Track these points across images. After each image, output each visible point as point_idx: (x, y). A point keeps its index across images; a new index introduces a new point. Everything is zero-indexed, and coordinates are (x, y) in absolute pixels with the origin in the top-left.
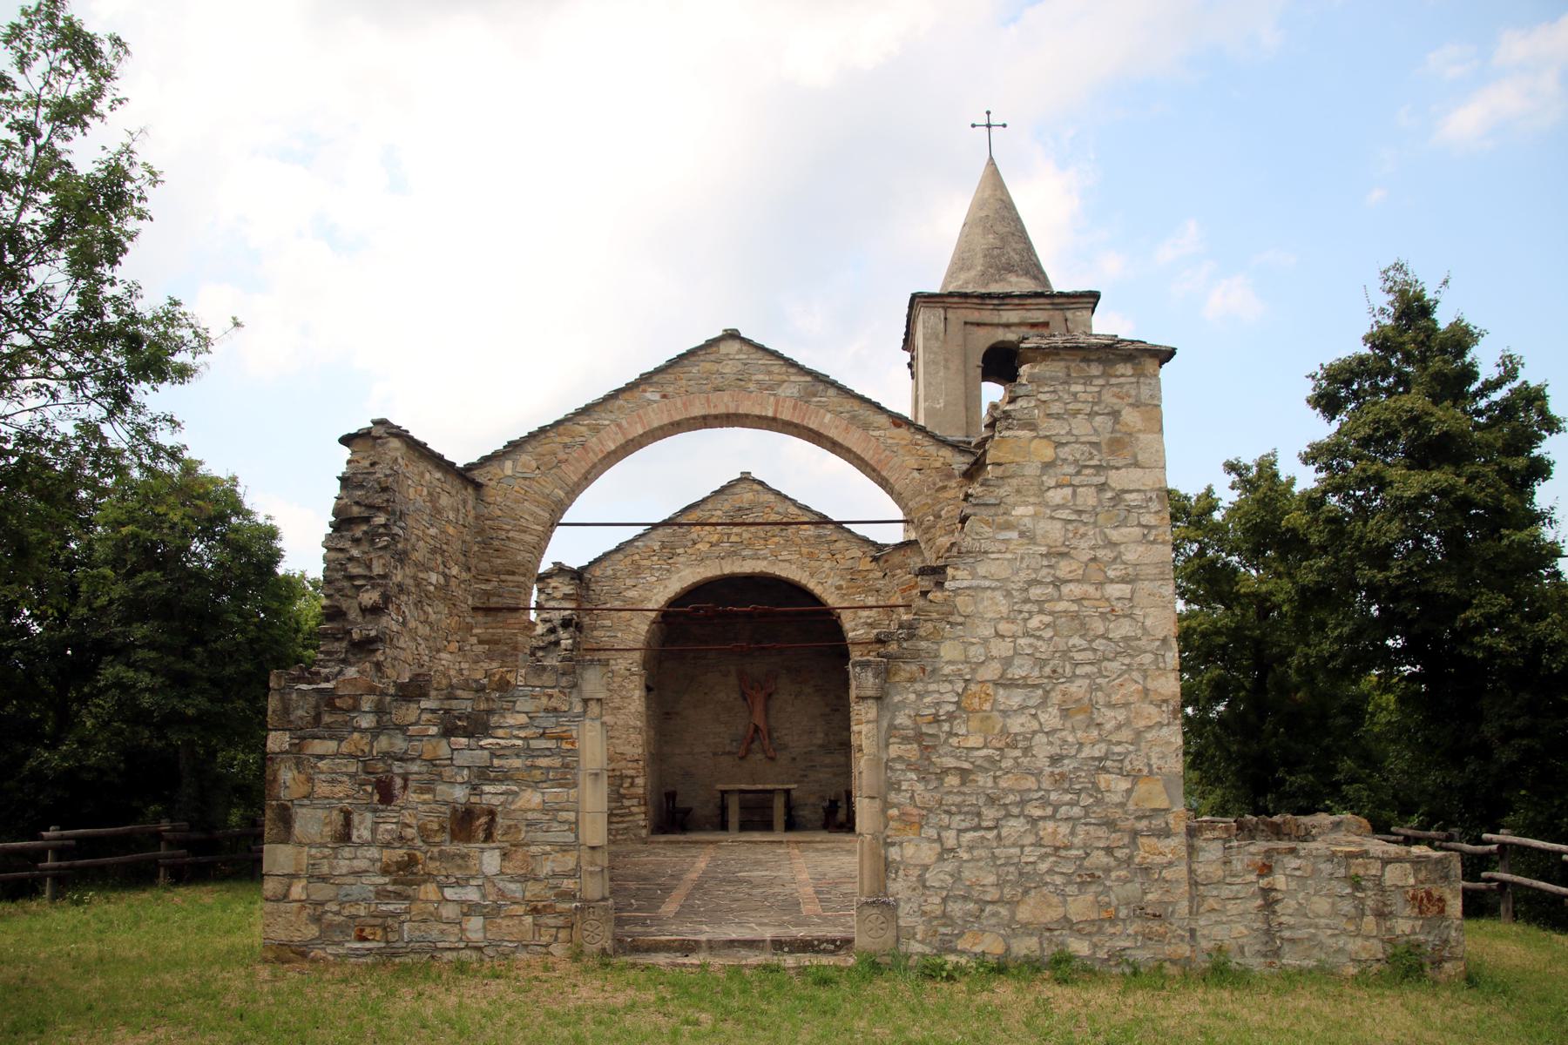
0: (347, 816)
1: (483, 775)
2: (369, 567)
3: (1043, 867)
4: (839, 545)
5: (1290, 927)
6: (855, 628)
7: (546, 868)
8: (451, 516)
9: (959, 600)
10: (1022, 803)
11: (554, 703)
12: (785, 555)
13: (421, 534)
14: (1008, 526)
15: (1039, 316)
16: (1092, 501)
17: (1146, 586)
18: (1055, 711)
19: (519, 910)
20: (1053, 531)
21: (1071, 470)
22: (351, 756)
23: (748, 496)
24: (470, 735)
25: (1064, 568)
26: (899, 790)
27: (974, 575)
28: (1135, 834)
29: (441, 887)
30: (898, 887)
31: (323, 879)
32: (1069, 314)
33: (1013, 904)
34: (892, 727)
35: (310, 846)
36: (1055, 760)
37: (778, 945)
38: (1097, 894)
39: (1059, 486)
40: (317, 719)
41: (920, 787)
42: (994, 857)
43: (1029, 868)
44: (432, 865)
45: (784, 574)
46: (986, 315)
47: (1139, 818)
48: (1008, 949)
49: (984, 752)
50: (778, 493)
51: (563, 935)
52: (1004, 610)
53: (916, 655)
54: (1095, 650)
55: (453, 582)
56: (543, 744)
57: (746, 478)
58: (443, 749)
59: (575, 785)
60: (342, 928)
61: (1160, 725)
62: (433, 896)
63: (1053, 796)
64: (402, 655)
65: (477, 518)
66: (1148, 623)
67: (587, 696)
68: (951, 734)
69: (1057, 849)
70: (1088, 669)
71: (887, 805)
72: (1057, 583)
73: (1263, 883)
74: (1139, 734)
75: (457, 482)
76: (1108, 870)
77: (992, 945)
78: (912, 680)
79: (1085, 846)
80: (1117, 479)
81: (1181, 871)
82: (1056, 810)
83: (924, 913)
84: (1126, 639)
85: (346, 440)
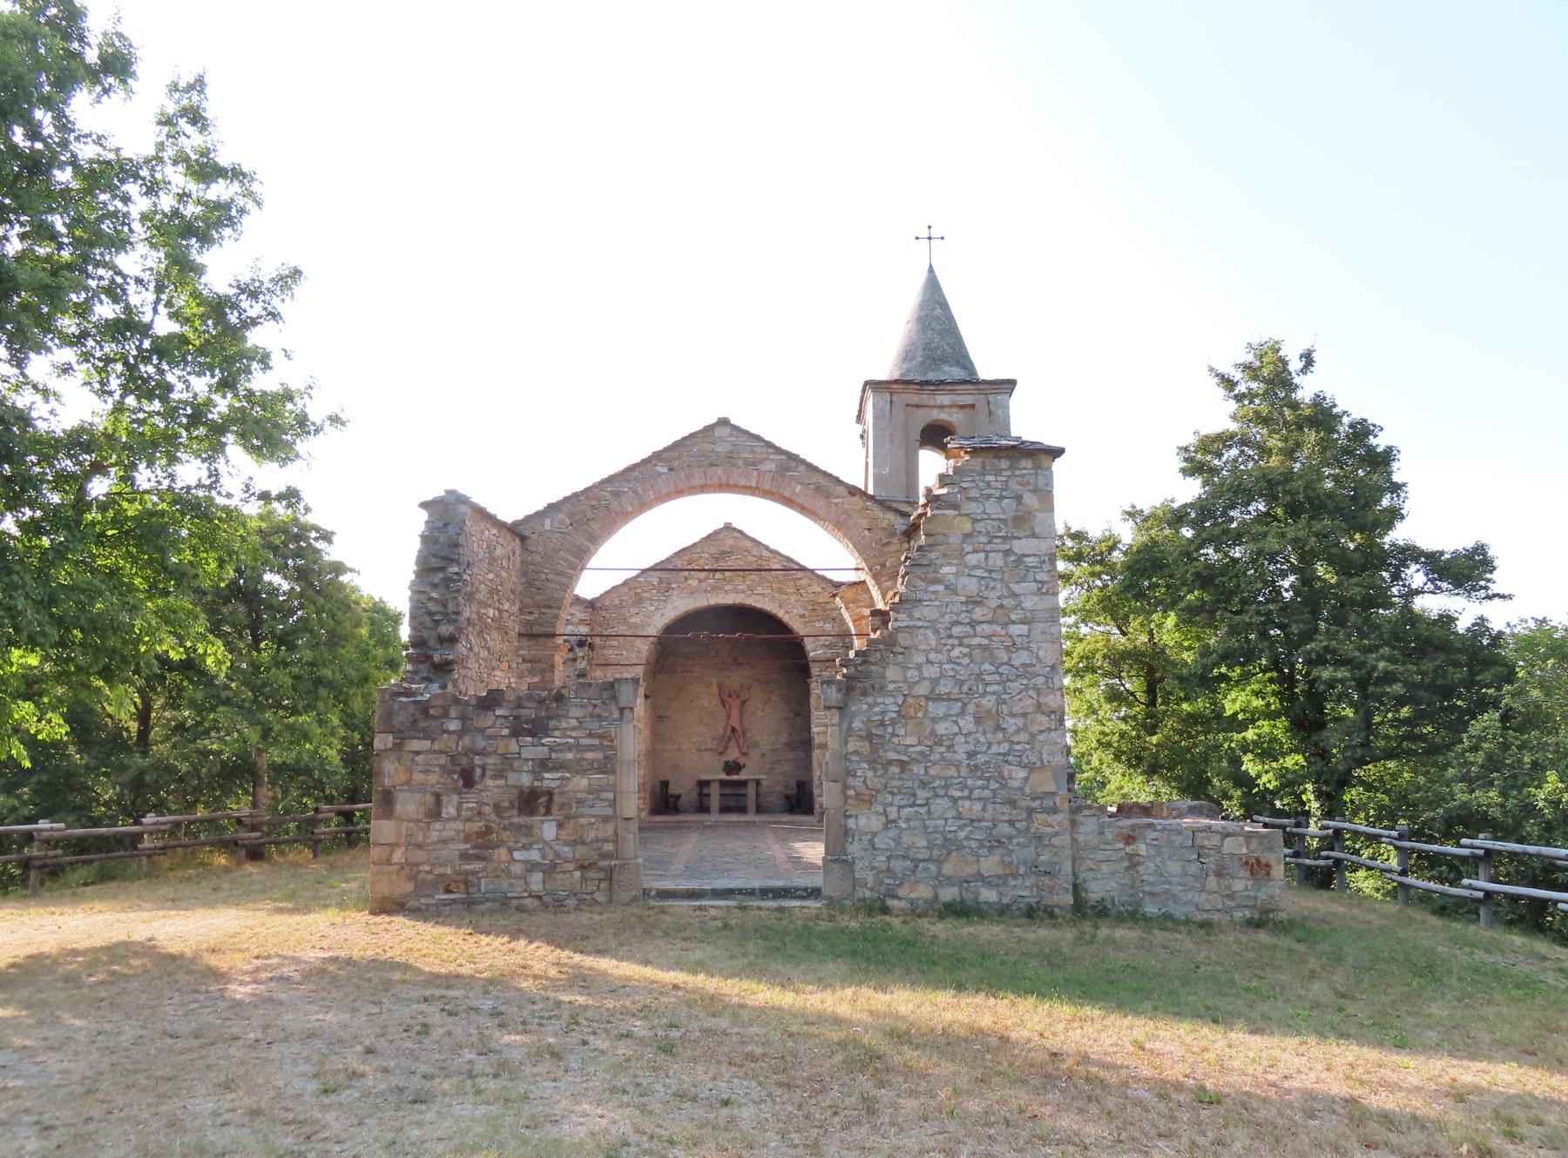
0: (438, 796)
1: (543, 765)
2: (445, 606)
3: (962, 834)
4: (804, 582)
5: (1151, 884)
6: (814, 649)
7: (591, 836)
8: (505, 563)
9: (900, 637)
10: (946, 787)
11: (598, 711)
12: (759, 590)
13: (481, 577)
14: (936, 581)
15: (967, 399)
16: (1000, 563)
17: (1041, 626)
18: (971, 719)
19: (570, 867)
20: (970, 585)
21: (984, 539)
22: (441, 752)
23: (730, 542)
24: (533, 735)
25: (978, 613)
26: (854, 776)
27: (911, 617)
28: (1030, 811)
29: (511, 850)
30: (854, 848)
31: (420, 847)
32: (991, 398)
33: (939, 862)
34: (850, 728)
35: (409, 820)
36: (971, 755)
37: (764, 893)
38: (1003, 856)
39: (975, 551)
40: (414, 722)
41: (870, 774)
42: (925, 827)
43: (951, 836)
44: (505, 835)
45: (758, 605)
46: (924, 398)
47: (1033, 799)
48: (936, 896)
49: (918, 748)
50: (754, 540)
51: (604, 885)
52: (933, 643)
53: (868, 676)
54: (1001, 674)
55: (505, 615)
56: (589, 741)
57: (728, 527)
58: (513, 746)
59: (613, 772)
60: (433, 885)
61: (1049, 730)
62: (504, 858)
63: (970, 782)
64: (469, 673)
65: (522, 562)
66: (1041, 653)
67: (622, 705)
68: (893, 735)
69: (972, 821)
70: (995, 688)
71: (846, 787)
72: (973, 624)
73: (1129, 849)
74: (1033, 736)
75: (508, 536)
76: (1010, 838)
77: (923, 892)
78: (864, 694)
79: (993, 820)
80: (1020, 546)
81: (1064, 840)
82: (971, 792)
83: (873, 868)
84: (1024, 665)
85: (424, 505)
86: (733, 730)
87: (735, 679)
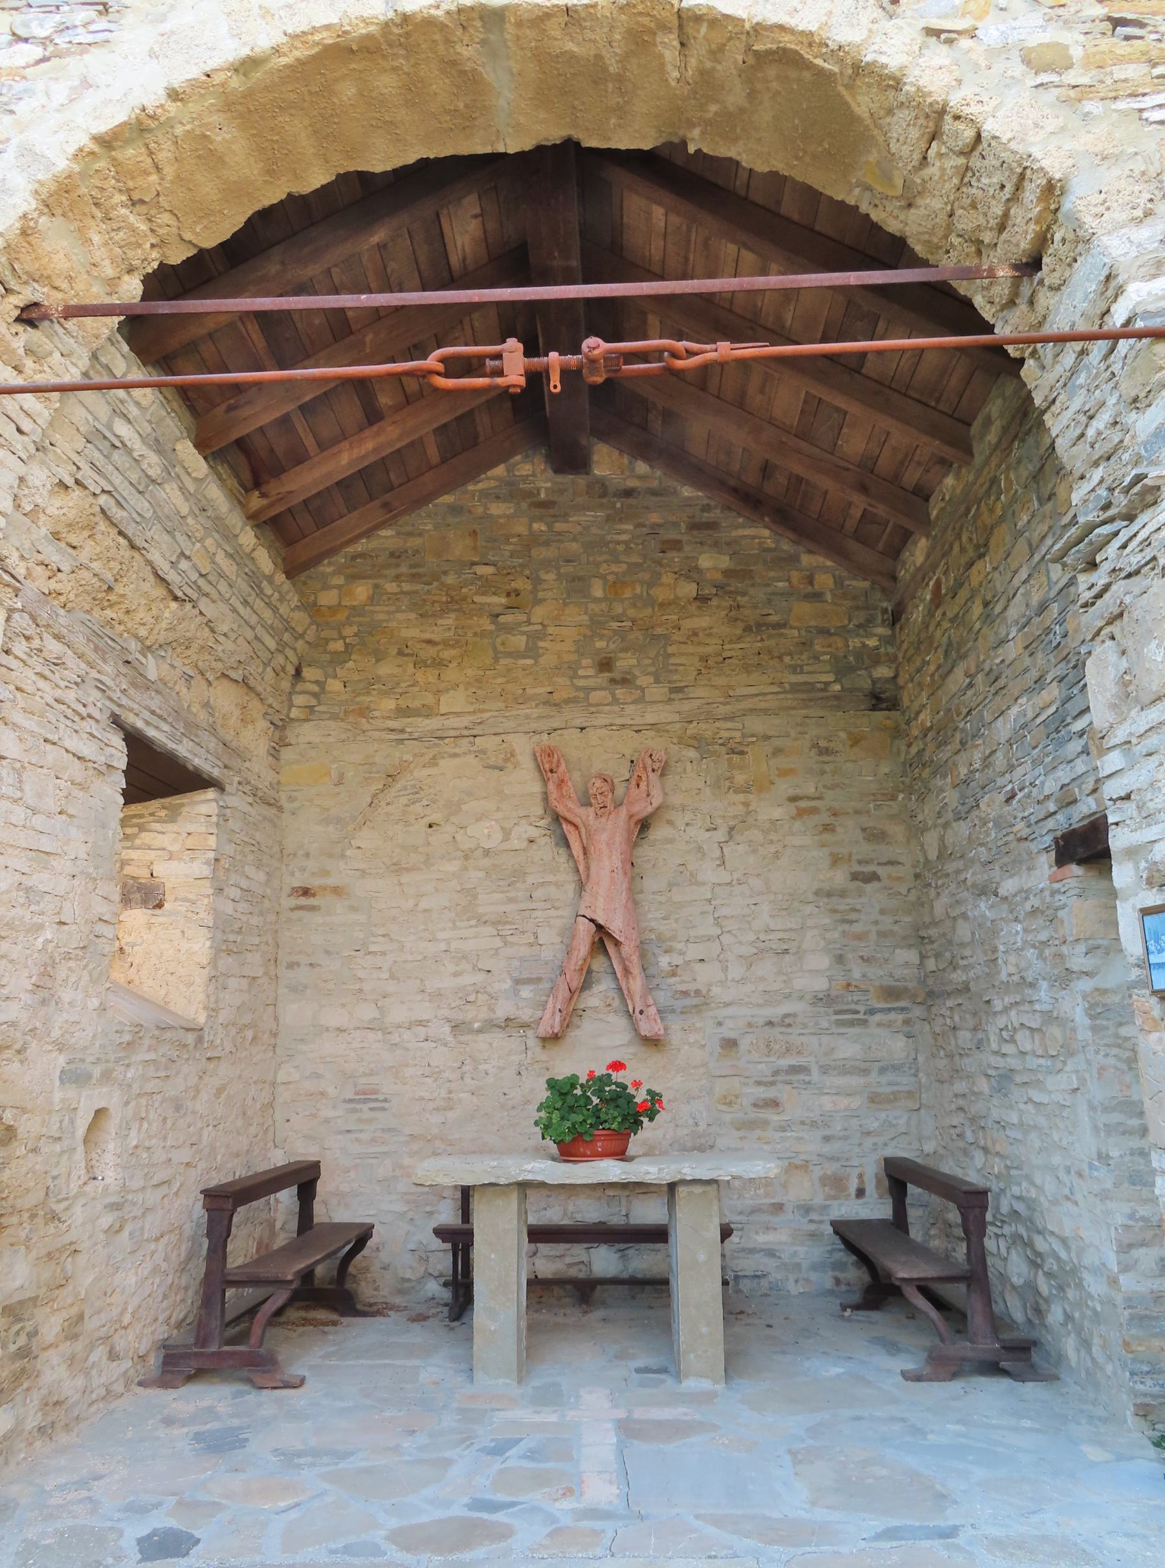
86: (602, 938)
87: (600, 746)
